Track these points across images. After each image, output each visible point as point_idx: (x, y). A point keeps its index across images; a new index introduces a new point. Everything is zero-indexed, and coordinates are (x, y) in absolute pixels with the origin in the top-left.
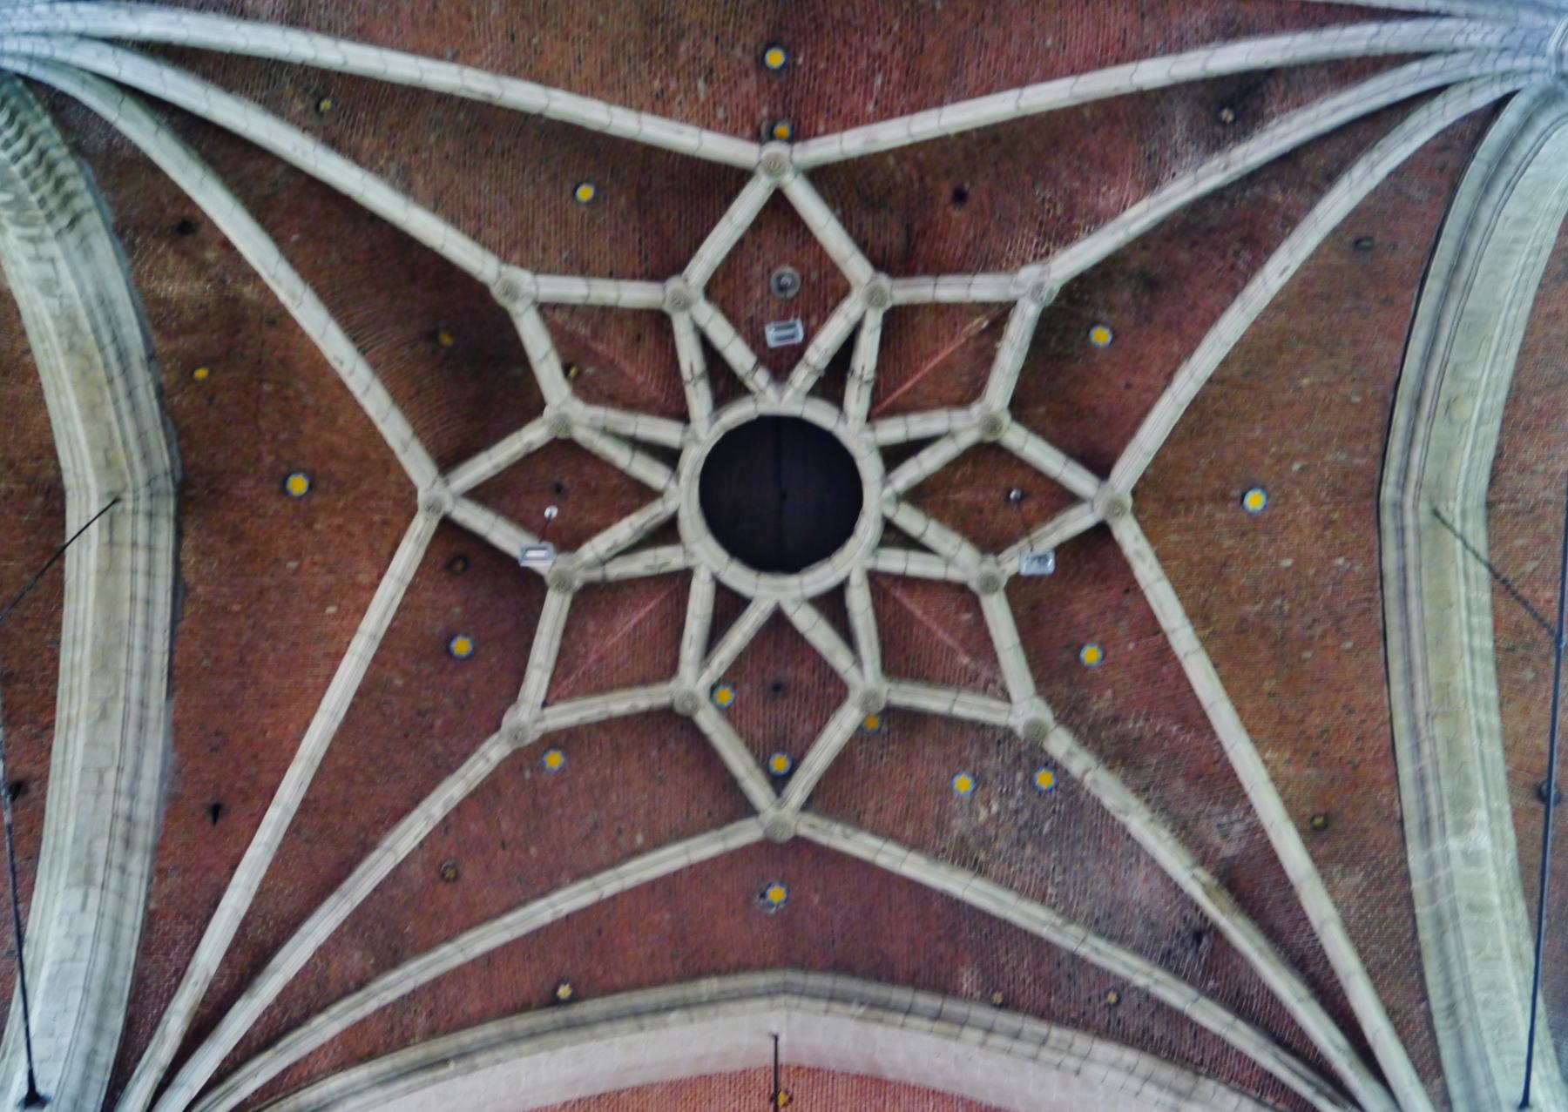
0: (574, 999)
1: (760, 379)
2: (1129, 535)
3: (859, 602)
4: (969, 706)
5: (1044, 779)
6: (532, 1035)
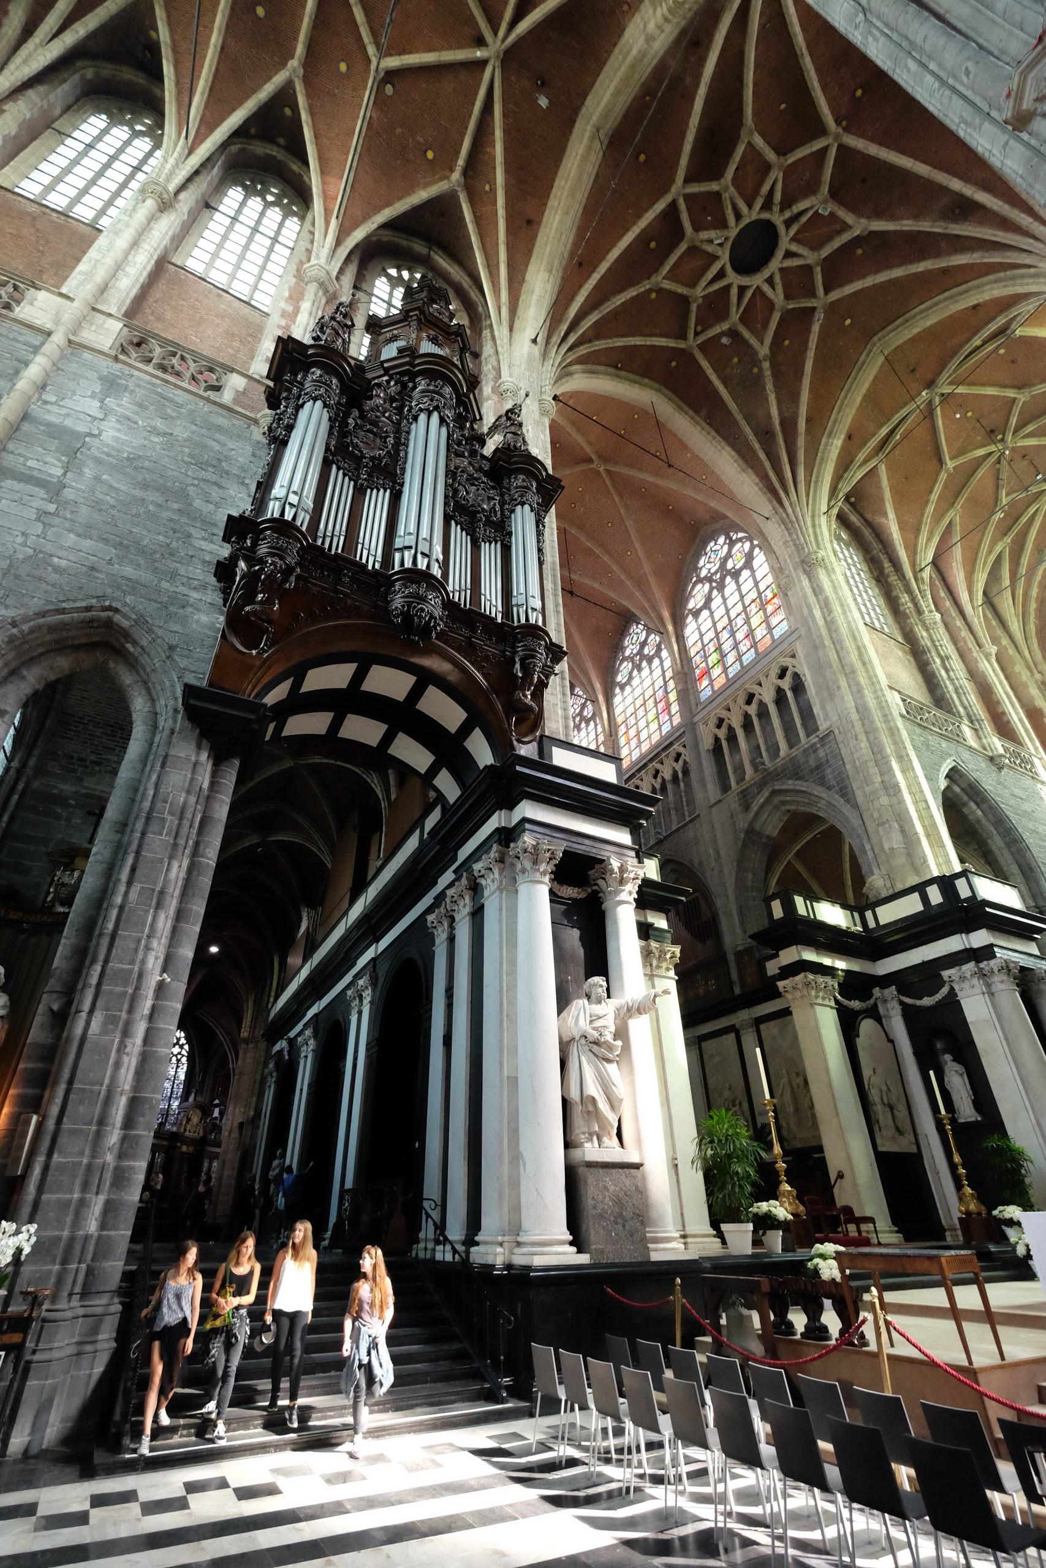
0: (620, 369)
1: (776, 208)
2: (819, 317)
3: (749, 294)
4: (753, 341)
5: (755, 370)
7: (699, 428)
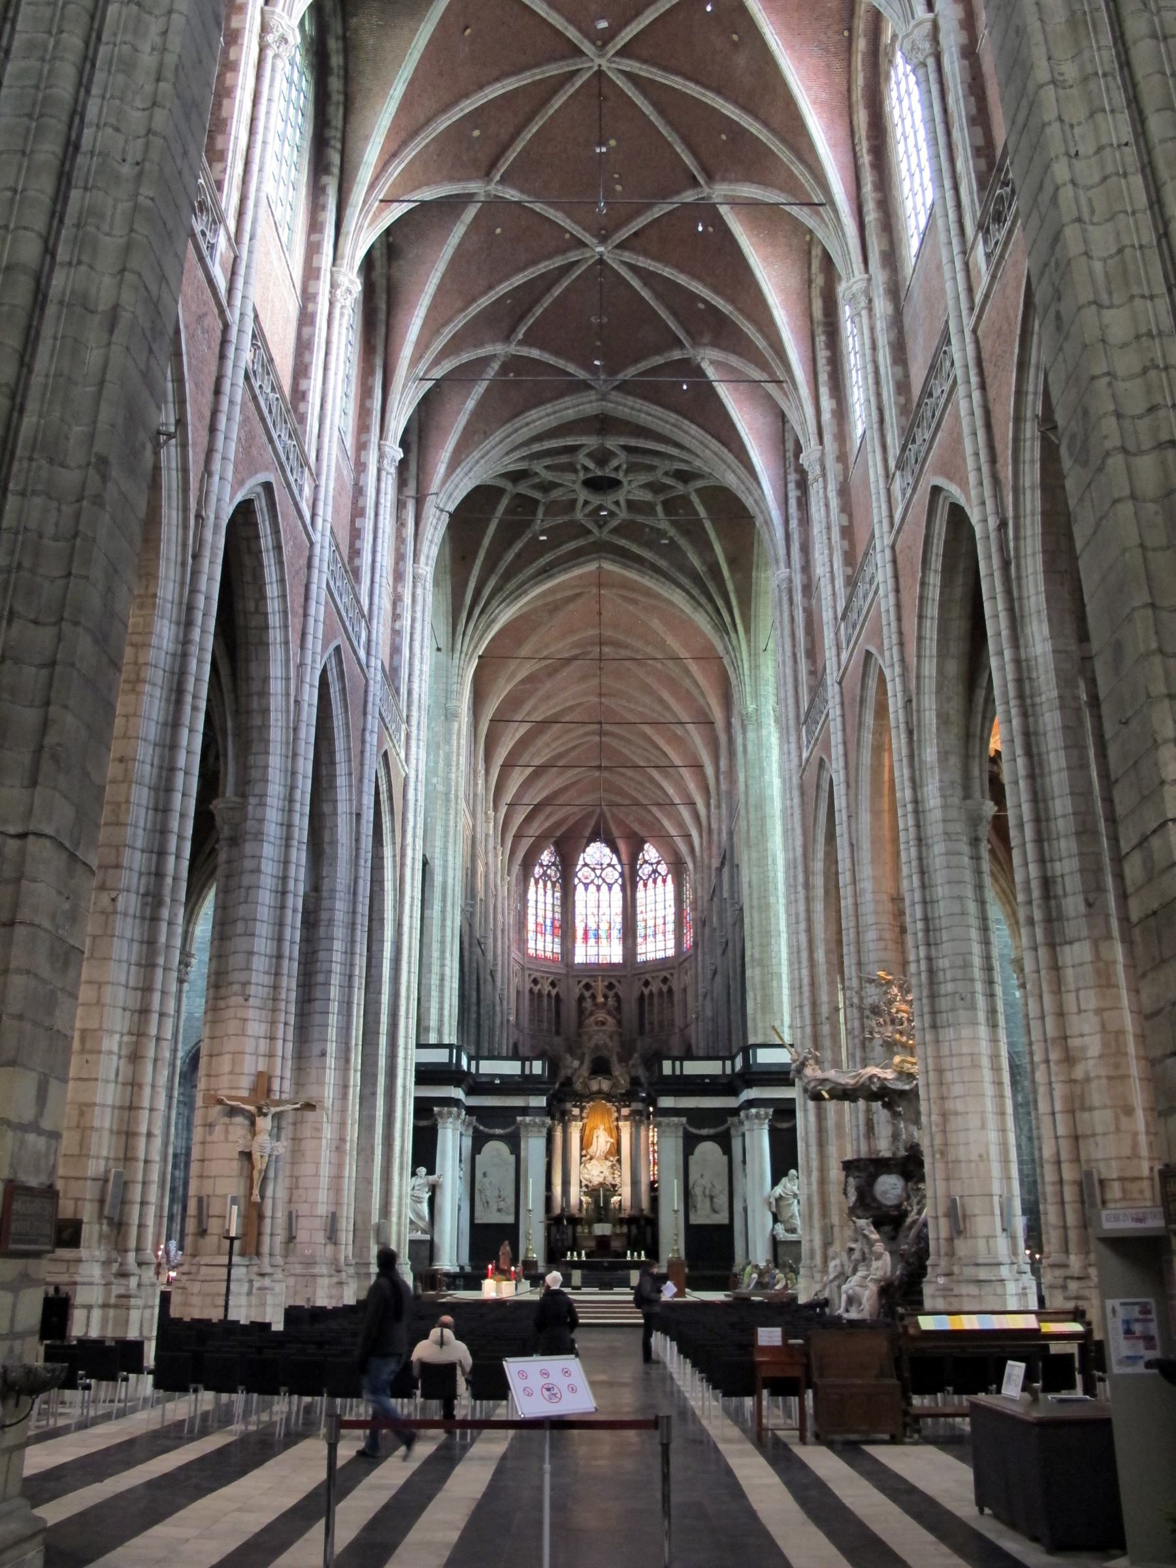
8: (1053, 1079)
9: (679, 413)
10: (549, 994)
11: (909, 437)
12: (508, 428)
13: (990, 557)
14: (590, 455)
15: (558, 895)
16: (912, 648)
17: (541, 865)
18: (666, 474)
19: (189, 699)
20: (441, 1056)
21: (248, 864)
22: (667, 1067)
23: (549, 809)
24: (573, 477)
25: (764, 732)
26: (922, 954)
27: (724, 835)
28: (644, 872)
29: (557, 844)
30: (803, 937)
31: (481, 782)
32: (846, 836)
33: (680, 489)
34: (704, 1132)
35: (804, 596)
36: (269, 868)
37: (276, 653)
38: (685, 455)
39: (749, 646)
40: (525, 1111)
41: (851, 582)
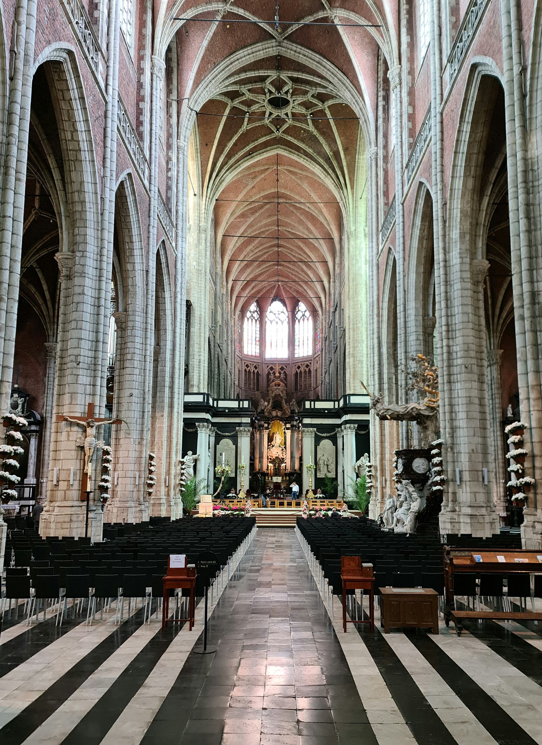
0: (252, 153)
6: (247, 160)
7: (302, 159)
8: (531, 409)
9: (321, 54)
10: (254, 372)
11: (457, 39)
12: (227, 61)
13: (513, 94)
14: (272, 83)
15: (258, 326)
16: (449, 172)
17: (250, 312)
18: (313, 96)
19: (13, 172)
20: (199, 399)
21: (77, 290)
22: (307, 405)
23: (253, 284)
24: (263, 97)
25: (359, 241)
26: (445, 343)
27: (337, 295)
28: (299, 315)
29: (257, 302)
30: (376, 341)
31: (219, 267)
32: (402, 286)
33: (320, 106)
34: (325, 435)
35: (384, 162)
36: (89, 292)
37: (87, 167)
38: (323, 83)
39: (353, 196)
40: (240, 424)
41: (412, 146)
